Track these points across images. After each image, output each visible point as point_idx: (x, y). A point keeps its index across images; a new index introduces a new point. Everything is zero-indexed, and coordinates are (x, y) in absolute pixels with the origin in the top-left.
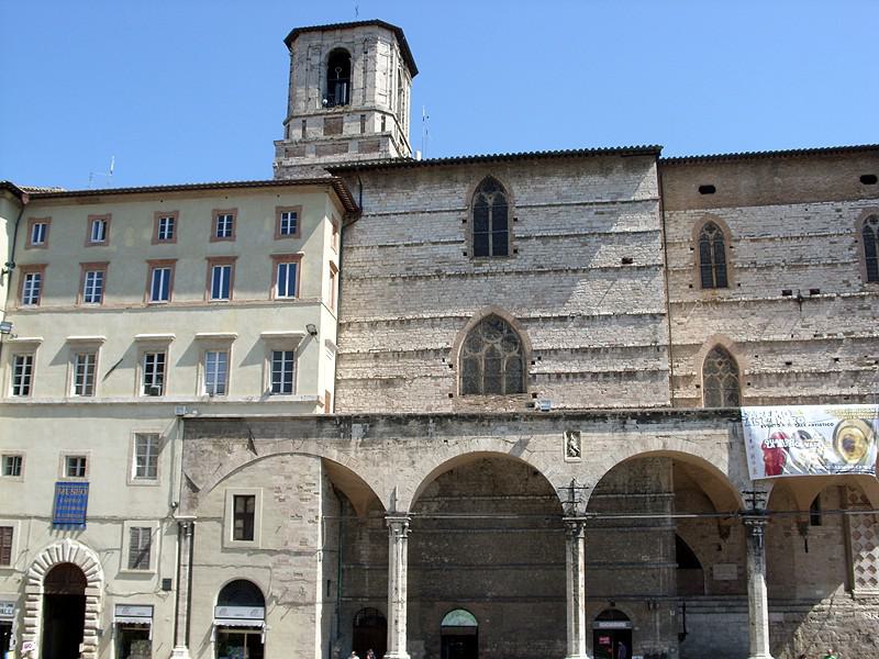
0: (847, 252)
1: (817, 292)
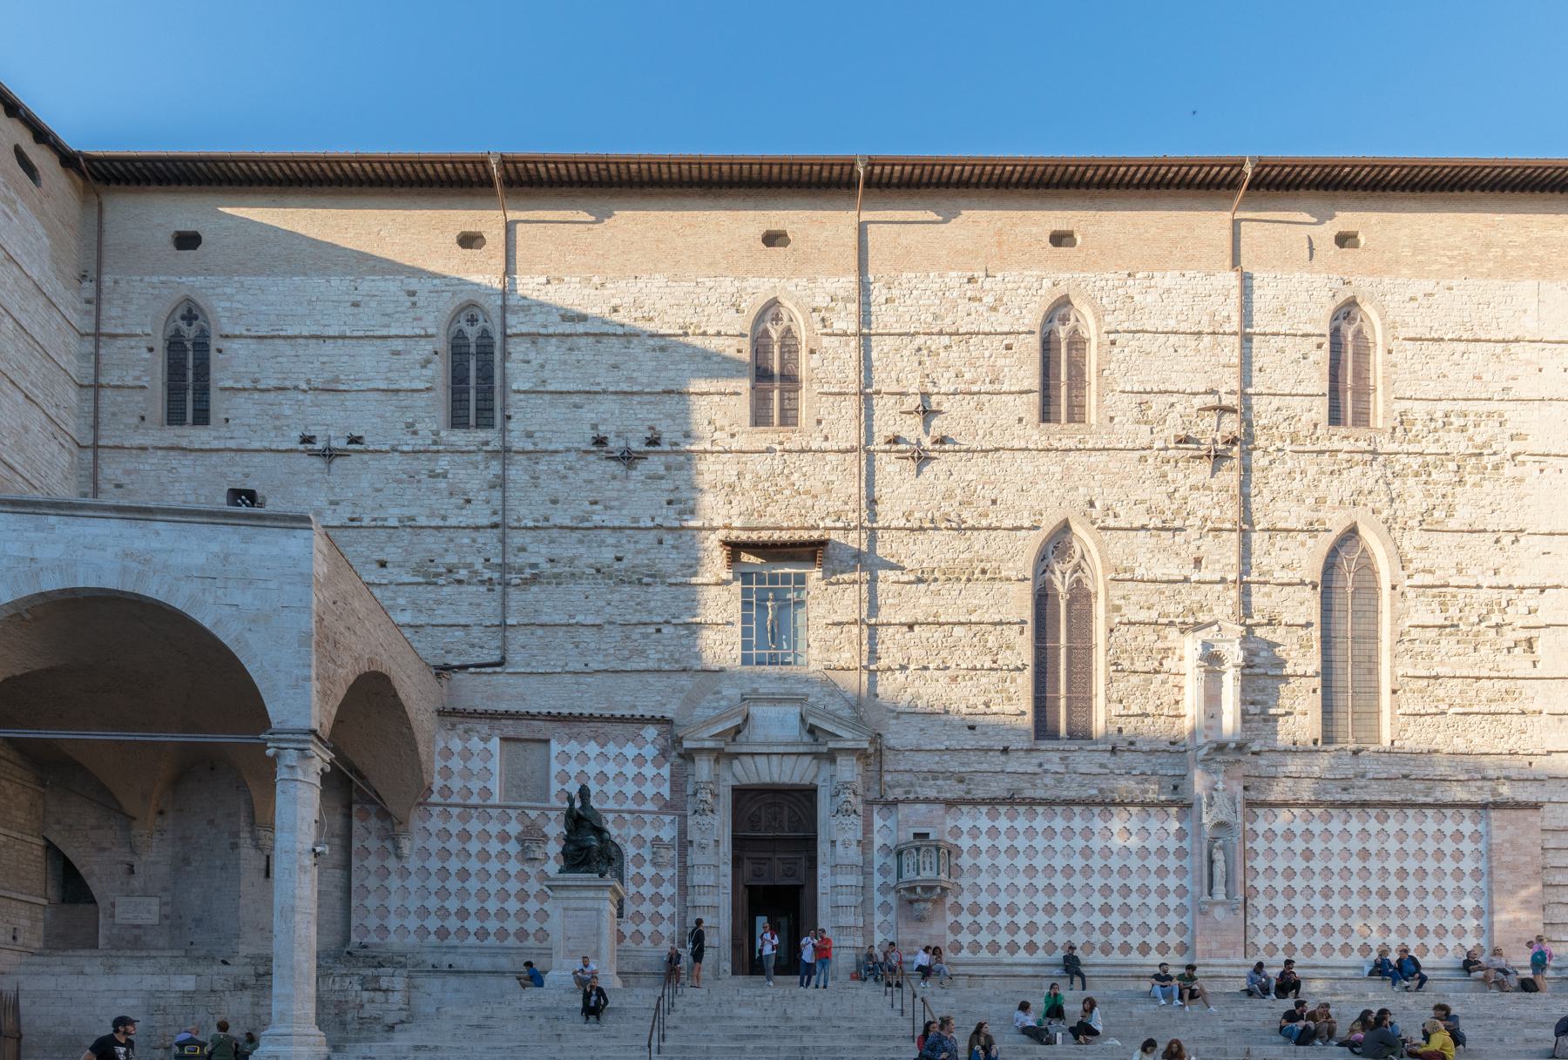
1: (354, 440)
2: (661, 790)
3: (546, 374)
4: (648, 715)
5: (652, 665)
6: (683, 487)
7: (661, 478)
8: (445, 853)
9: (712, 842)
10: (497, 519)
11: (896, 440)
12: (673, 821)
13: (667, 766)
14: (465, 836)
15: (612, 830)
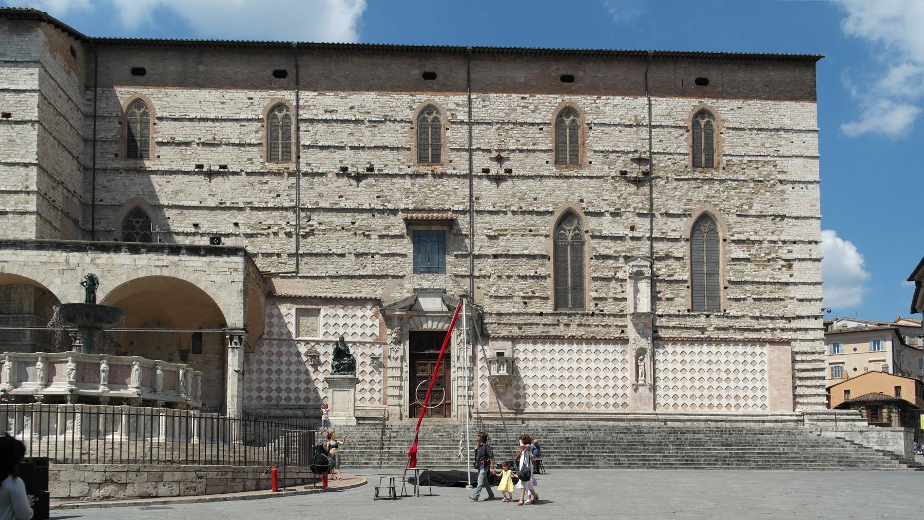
0: (253, 135)
1: (224, 167)
3: (318, 137)
4: (368, 296)
5: (370, 273)
7: (375, 185)
8: (270, 362)
10: (293, 204)
11: (486, 171)
14: (280, 354)
15: (351, 351)
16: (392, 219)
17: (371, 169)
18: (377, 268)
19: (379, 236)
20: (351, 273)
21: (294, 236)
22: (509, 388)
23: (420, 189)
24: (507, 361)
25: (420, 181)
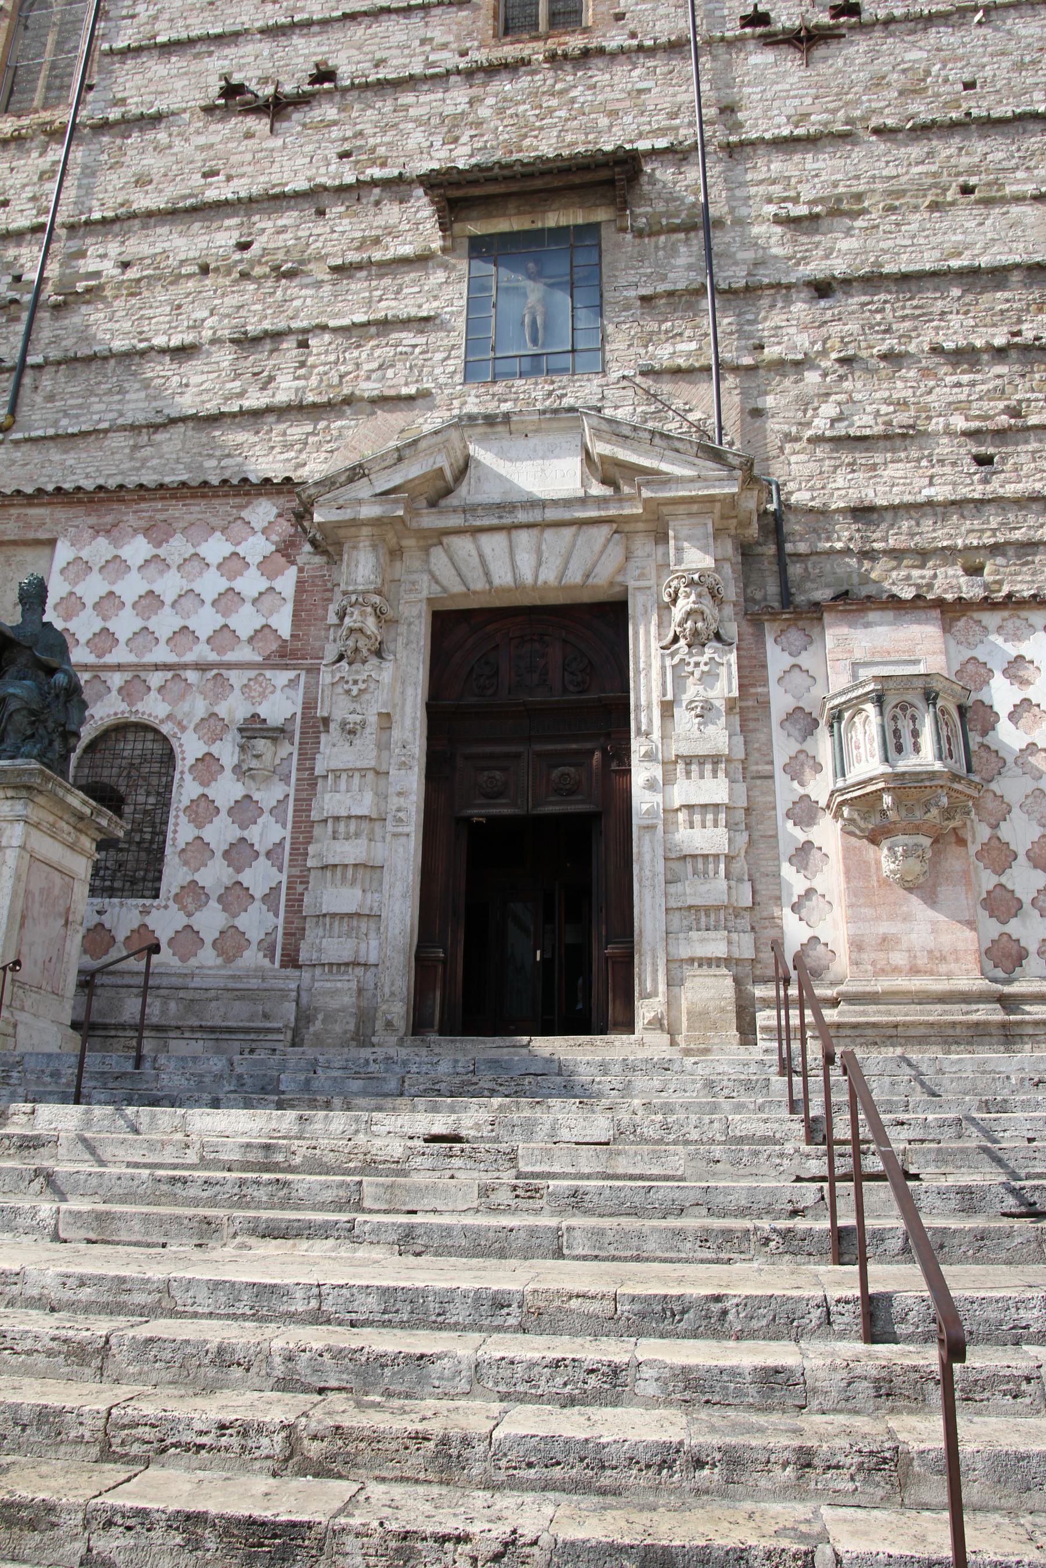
2: (274, 622)
5: (282, 397)
6: (369, 131)
7: (335, 123)
9: (373, 719)
12: (292, 683)
13: (292, 572)
16: (391, 213)
17: (324, 75)
18: (314, 381)
19: (335, 269)
20: (211, 407)
21: (25, 316)
22: (954, 861)
23: (500, 111)
24: (930, 697)
25: (505, 86)
